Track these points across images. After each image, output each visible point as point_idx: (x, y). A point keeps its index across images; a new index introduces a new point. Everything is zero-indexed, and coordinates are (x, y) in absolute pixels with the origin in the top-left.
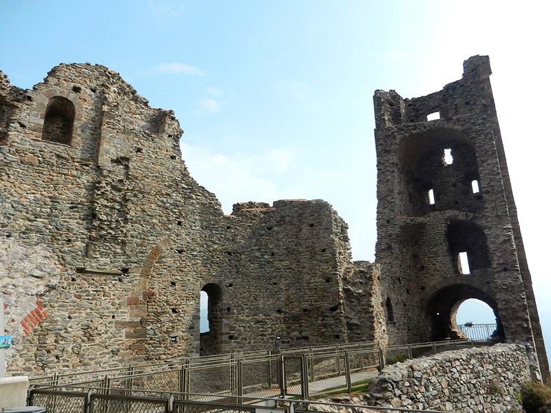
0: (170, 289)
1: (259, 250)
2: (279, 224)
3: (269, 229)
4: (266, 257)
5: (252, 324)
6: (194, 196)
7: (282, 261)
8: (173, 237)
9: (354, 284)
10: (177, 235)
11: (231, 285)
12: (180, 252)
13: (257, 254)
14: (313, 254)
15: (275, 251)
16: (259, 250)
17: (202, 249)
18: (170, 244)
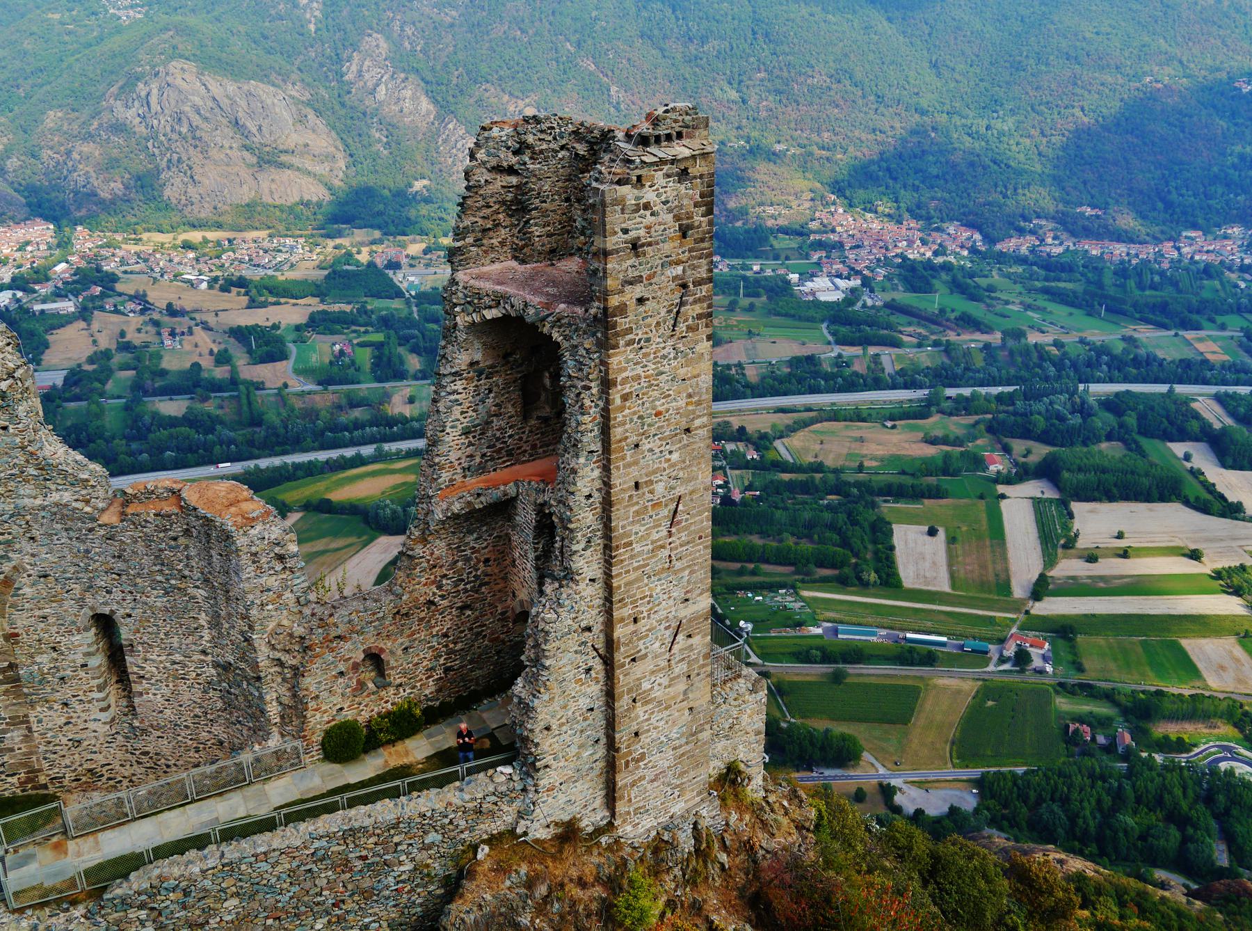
0: (42, 625)
1: (161, 571)
2: (187, 533)
3: (175, 539)
4: (173, 582)
5: (168, 665)
6: (53, 487)
7: (197, 587)
8: (27, 559)
9: (288, 651)
10: (33, 555)
11: (129, 616)
12: (45, 576)
13: (159, 578)
14: (228, 599)
15: (187, 573)
16: (161, 571)
17: (77, 568)
18: (25, 570)
